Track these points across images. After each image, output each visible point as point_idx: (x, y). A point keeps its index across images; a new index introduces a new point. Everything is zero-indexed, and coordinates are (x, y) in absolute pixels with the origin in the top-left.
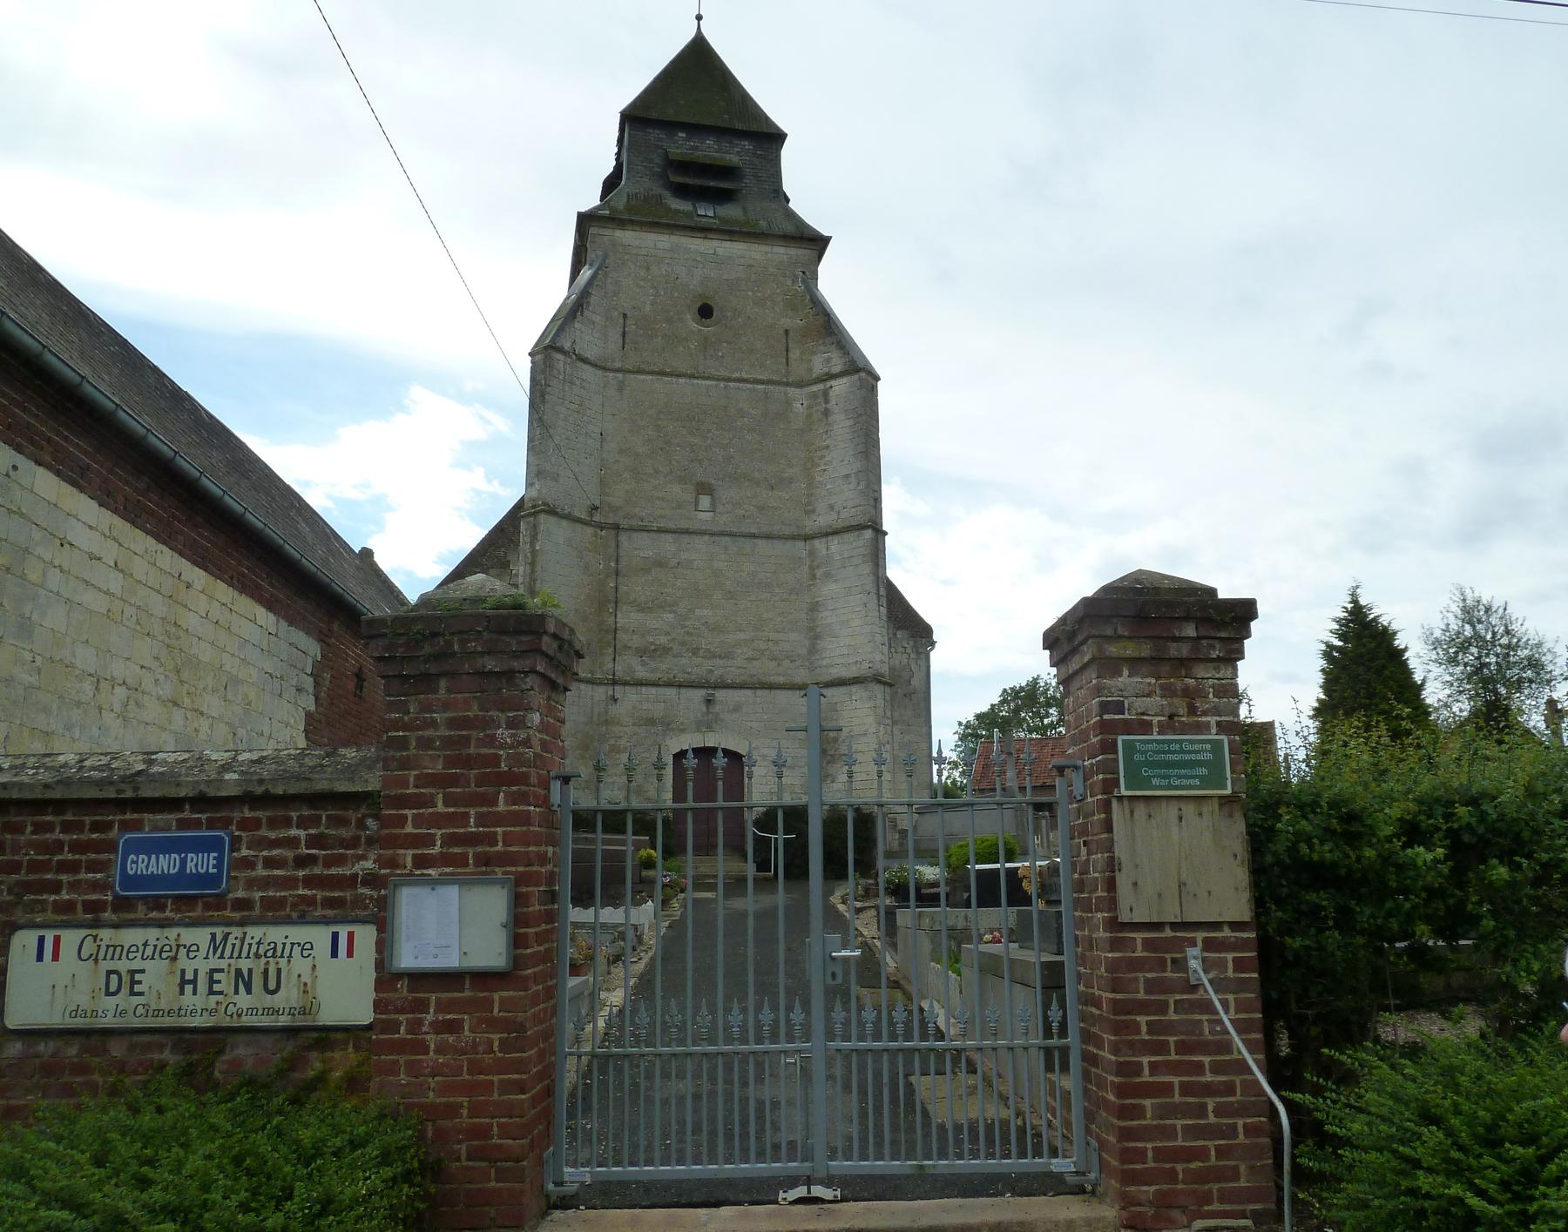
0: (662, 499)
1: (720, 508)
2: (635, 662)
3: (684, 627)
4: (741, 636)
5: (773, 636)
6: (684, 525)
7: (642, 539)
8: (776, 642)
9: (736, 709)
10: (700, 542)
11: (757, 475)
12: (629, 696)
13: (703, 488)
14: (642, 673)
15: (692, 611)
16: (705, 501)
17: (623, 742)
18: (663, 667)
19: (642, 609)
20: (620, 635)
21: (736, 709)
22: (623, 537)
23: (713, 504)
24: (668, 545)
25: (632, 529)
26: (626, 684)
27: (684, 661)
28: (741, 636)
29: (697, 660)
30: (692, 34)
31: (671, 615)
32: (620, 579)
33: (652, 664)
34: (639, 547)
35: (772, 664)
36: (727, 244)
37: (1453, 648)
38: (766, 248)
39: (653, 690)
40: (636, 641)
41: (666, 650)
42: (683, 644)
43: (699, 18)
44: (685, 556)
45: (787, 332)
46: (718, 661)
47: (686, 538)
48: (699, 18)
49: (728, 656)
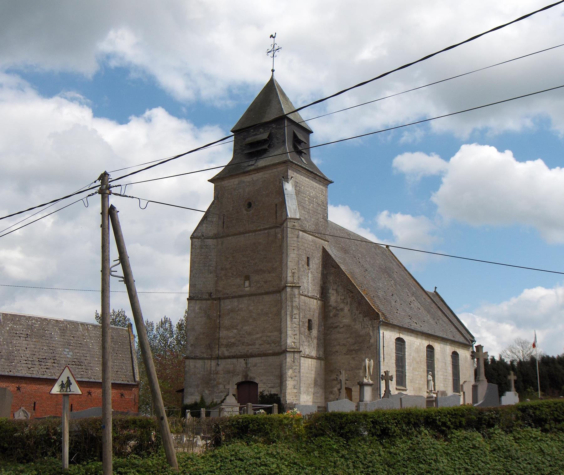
0: (234, 285)
1: (252, 285)
2: (224, 349)
3: (239, 334)
4: (258, 336)
5: (269, 334)
6: (240, 293)
7: (227, 302)
8: (269, 337)
9: (255, 365)
10: (245, 300)
11: (265, 269)
12: (223, 363)
13: (247, 278)
14: (227, 354)
15: (242, 328)
16: (247, 284)
17: (220, 380)
18: (234, 351)
19: (228, 329)
20: (221, 340)
21: (255, 365)
22: (222, 301)
23: (250, 285)
24: (235, 302)
25: (224, 299)
26: (221, 358)
27: (240, 348)
28: (258, 336)
29: (244, 347)
30: (268, 80)
31: (236, 331)
32: (221, 319)
33: (230, 350)
34: (227, 305)
35: (268, 346)
36: (257, 175)
37: (261, 393)
38: (270, 171)
39: (229, 360)
40: (224, 342)
41: (234, 344)
42: (239, 341)
43: (273, 71)
44: (240, 306)
45: (276, 205)
46: (250, 347)
47: (241, 299)
48: (273, 71)
49: (254, 344)
